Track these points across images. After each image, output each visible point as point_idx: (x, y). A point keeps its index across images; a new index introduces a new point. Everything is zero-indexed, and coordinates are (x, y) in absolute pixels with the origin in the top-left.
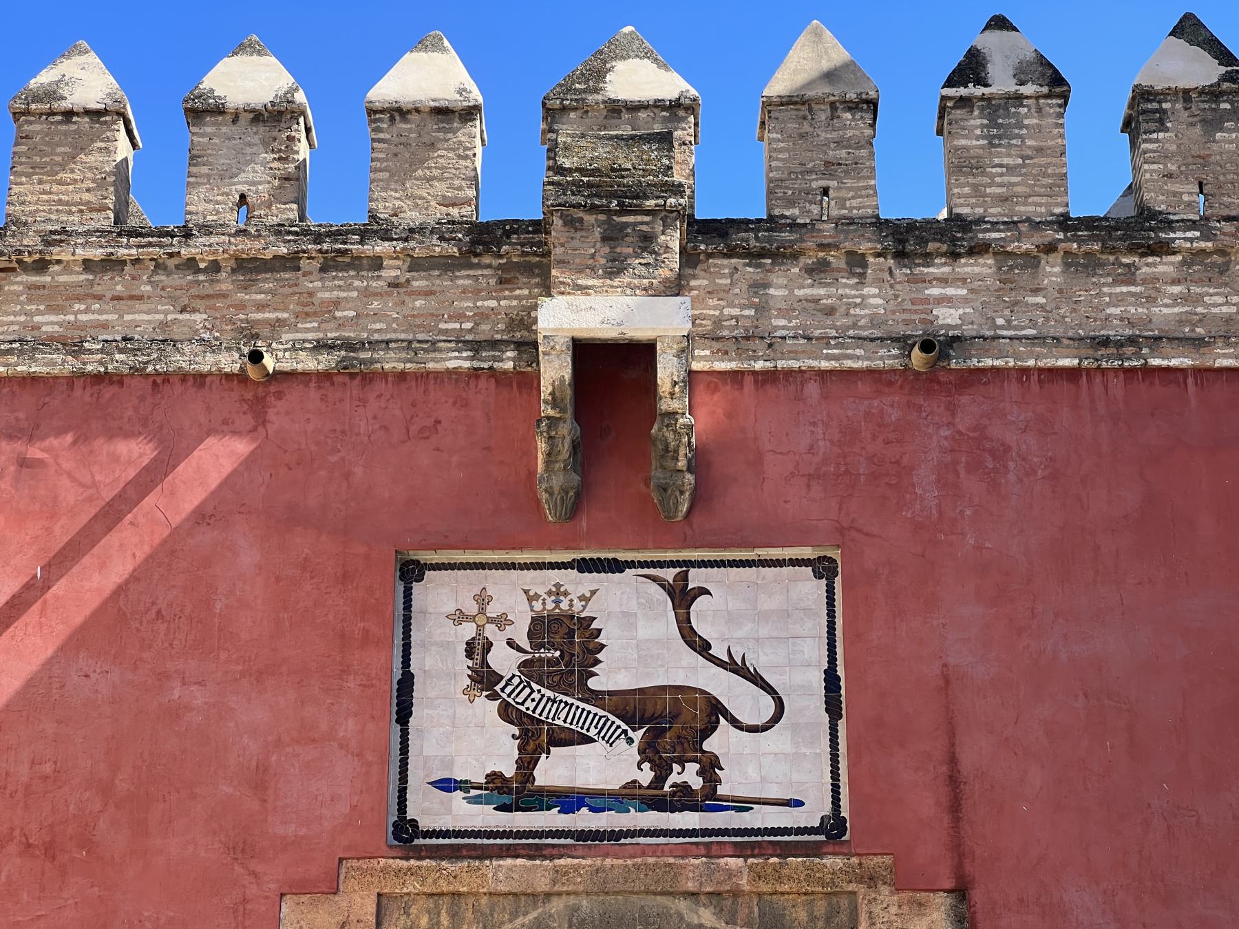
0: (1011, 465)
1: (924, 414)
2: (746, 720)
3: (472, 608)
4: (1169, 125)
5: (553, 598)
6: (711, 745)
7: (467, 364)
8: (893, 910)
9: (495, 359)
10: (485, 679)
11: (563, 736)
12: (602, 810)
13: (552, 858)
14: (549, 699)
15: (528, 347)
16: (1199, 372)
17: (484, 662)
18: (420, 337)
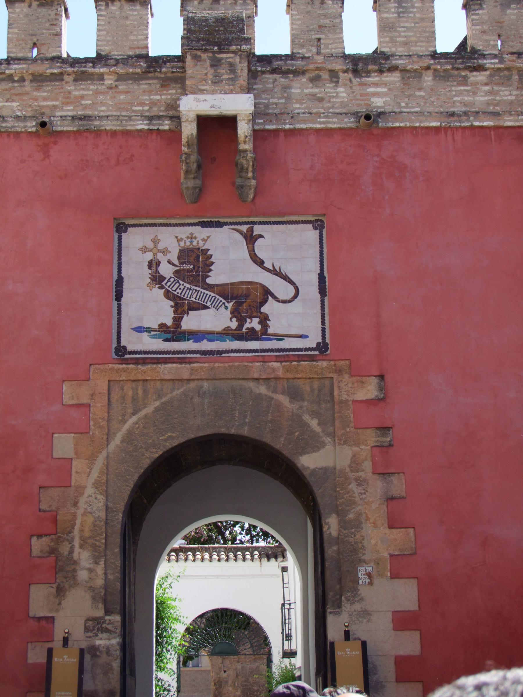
0: (407, 174)
1: (366, 150)
2: (281, 297)
3: (151, 245)
4: (484, 6)
5: (189, 240)
6: (265, 309)
7: (146, 127)
8: (350, 385)
9: (160, 125)
10: (157, 279)
11: (195, 306)
12: (214, 341)
13: (190, 363)
14: (188, 288)
15: (177, 119)
16: (497, 128)
17: (157, 271)
18: (124, 114)
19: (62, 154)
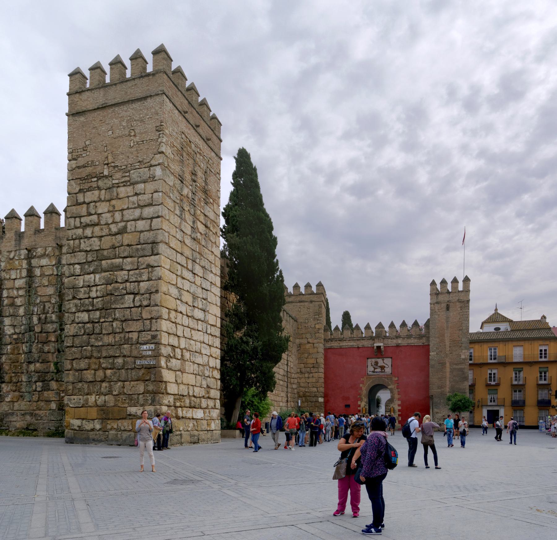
19: (360, 350)
